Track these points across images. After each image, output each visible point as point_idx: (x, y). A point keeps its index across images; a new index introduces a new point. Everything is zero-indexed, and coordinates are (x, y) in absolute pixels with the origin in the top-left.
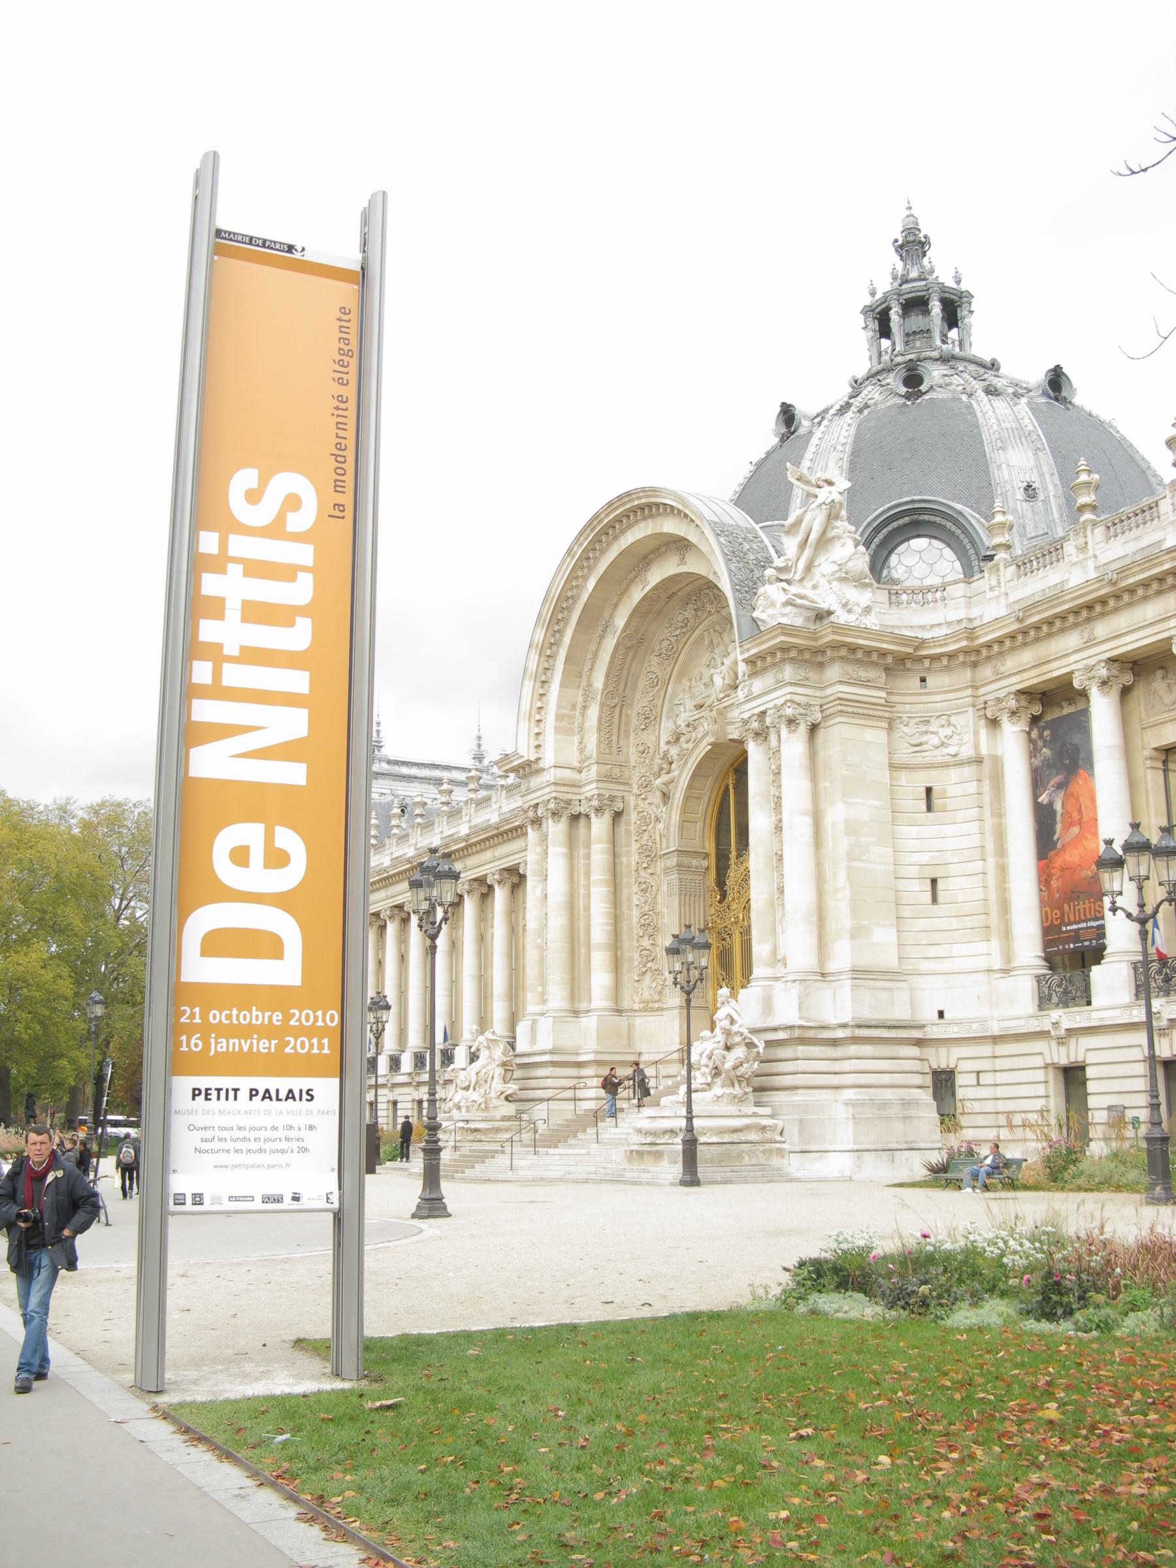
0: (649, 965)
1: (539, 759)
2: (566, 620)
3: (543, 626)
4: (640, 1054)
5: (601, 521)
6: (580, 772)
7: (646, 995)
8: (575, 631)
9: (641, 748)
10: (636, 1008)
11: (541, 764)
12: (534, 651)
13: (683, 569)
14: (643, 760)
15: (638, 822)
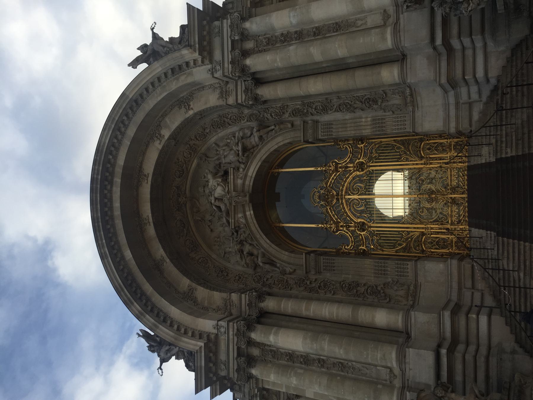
0: (379, 288)
1: (208, 336)
2: (139, 287)
3: (132, 304)
4: (449, 301)
5: (98, 219)
6: (231, 314)
7: (402, 293)
8: (148, 281)
9: (237, 278)
10: (411, 303)
11: (212, 336)
12: (142, 317)
13: (150, 179)
14: (244, 279)
15: (280, 285)
